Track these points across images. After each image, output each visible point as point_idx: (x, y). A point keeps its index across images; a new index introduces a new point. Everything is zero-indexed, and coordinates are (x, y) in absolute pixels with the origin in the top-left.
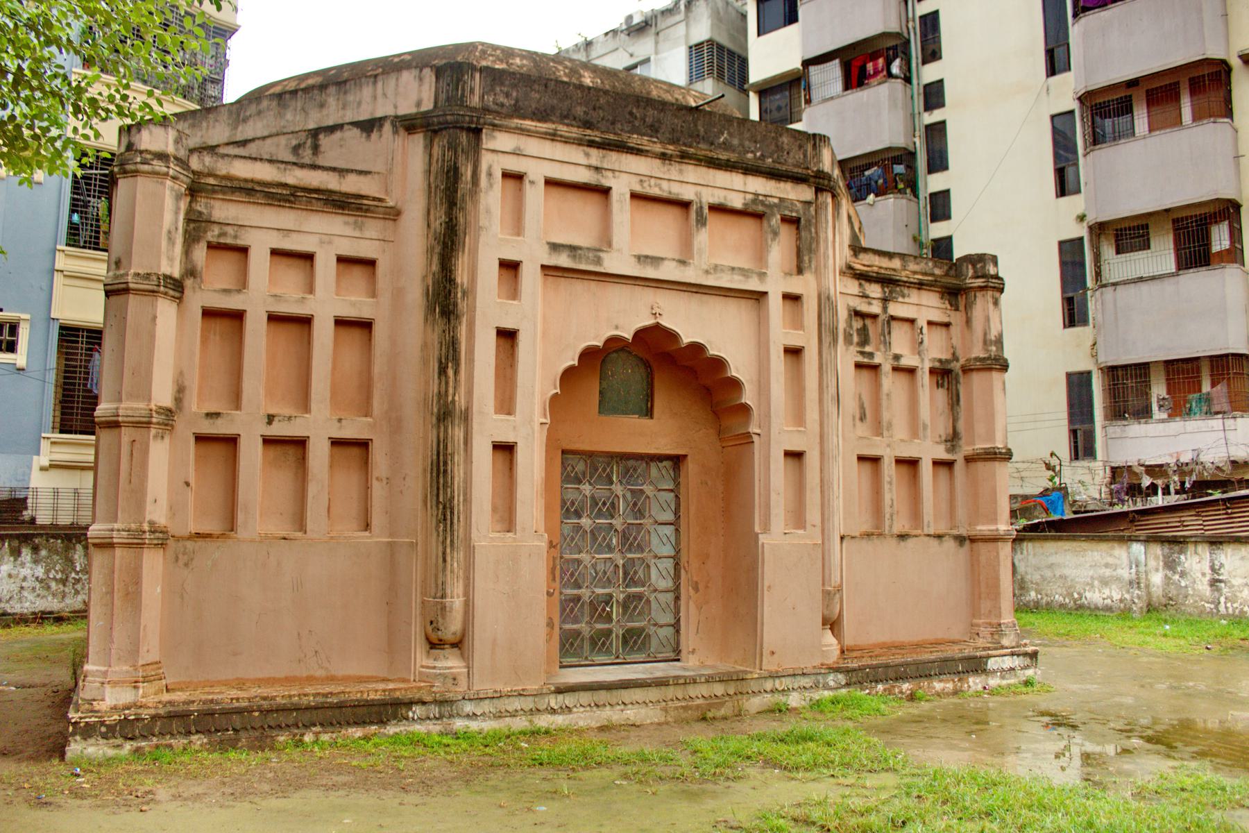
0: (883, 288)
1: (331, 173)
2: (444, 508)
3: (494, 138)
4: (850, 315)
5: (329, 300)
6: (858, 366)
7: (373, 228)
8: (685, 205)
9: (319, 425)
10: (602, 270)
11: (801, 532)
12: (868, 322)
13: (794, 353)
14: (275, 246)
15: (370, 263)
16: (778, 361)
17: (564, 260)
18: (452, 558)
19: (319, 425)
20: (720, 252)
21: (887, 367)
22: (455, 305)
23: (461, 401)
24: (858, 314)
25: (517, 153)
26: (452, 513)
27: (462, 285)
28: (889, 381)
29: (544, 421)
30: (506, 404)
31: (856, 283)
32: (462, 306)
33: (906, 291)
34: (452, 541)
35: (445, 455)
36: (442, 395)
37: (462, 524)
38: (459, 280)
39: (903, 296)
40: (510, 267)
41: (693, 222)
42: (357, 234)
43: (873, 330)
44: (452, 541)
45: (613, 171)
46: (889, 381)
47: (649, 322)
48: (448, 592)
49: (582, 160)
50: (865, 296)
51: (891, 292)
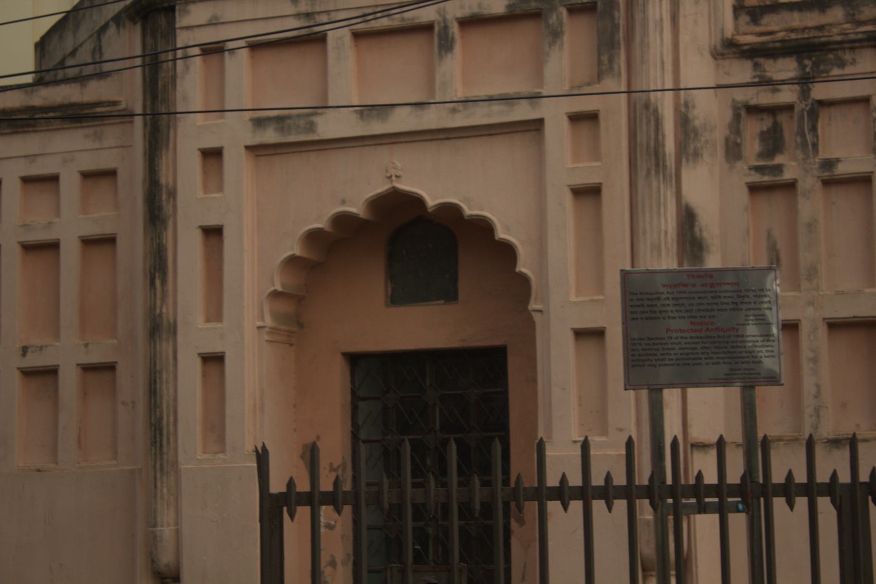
0: (800, 61)
1: (73, 85)
2: (155, 430)
3: (187, 12)
4: (737, 117)
5: (71, 220)
6: (754, 189)
7: (112, 134)
8: (428, 28)
9: (68, 353)
10: (316, 138)
11: (604, 439)
12: (783, 118)
13: (588, 193)
14: (24, 174)
15: (111, 174)
16: (562, 210)
17: (270, 136)
18: (162, 483)
19: (68, 353)
20: (475, 75)
21: (809, 182)
22: (160, 208)
23: (167, 311)
24: (753, 110)
25: (214, 23)
26: (161, 434)
27: (167, 186)
28: (812, 203)
29: (261, 324)
30: (215, 310)
31: (748, 64)
32: (167, 208)
33: (848, 56)
34: (161, 465)
35: (155, 373)
36: (152, 308)
37: (172, 445)
38: (163, 181)
39: (842, 65)
40: (212, 156)
41: (436, 50)
42: (97, 145)
43: (789, 127)
44: (161, 465)
45: (328, 12)
46: (812, 203)
47: (381, 188)
48: (159, 519)
49: (290, 10)
50: (765, 82)
51: (816, 65)
